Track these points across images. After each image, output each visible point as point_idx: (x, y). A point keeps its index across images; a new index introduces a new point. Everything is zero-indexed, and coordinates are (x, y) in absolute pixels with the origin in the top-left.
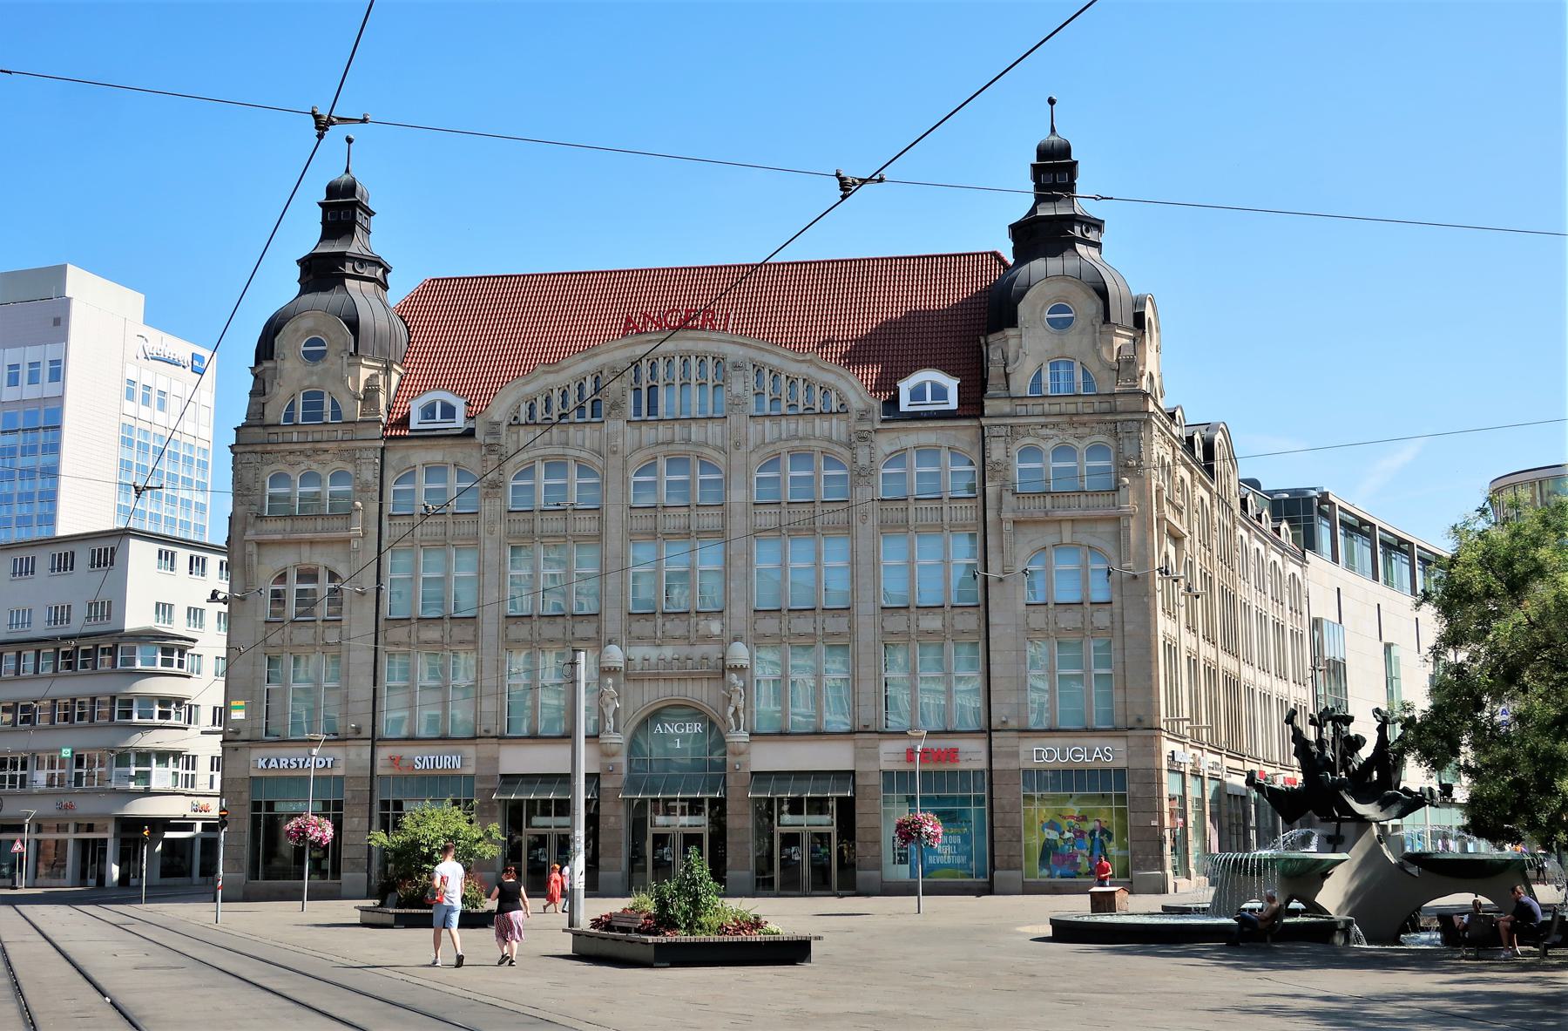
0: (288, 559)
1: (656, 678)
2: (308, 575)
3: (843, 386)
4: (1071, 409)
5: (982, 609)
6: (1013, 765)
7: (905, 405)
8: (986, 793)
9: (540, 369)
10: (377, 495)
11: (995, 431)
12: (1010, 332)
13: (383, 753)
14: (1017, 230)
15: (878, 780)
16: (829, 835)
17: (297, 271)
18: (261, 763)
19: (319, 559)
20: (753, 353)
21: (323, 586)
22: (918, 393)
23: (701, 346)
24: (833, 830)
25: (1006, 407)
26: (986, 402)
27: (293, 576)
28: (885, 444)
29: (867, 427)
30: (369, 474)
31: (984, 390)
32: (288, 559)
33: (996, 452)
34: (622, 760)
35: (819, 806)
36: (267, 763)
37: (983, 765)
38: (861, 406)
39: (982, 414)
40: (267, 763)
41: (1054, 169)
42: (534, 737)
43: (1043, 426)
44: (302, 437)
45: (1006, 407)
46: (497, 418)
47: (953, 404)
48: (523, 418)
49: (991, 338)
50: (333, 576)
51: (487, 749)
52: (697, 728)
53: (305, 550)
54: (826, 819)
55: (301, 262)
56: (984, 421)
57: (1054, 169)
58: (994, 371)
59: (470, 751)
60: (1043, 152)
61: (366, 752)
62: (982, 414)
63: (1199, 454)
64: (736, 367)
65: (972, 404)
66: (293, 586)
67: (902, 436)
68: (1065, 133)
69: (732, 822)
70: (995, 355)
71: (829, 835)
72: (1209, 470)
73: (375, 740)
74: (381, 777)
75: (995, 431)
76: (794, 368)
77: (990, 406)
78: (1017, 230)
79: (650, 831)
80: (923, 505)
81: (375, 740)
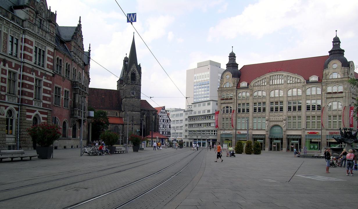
0: (225, 105)
1: (273, 121)
2: (227, 107)
3: (300, 78)
4: (336, 80)
6: (325, 134)
8: (321, 138)
10: (236, 96)
11: (324, 84)
12: (327, 69)
13: (237, 131)
14: (329, 52)
17: (226, 66)
18: (222, 132)
19: (229, 105)
20: (287, 74)
21: (229, 109)
23: (280, 73)
25: (326, 81)
27: (225, 108)
28: (307, 87)
29: (304, 84)
30: (235, 94)
32: (225, 105)
33: (324, 87)
34: (268, 133)
37: (321, 134)
41: (336, 41)
42: (257, 130)
43: (332, 83)
44: (226, 89)
45: (326, 81)
46: (252, 85)
50: (231, 108)
52: (279, 128)
53: (227, 104)
54: (298, 141)
55: (226, 65)
58: (324, 76)
60: (334, 39)
64: (285, 76)
65: (320, 81)
66: (225, 109)
67: (310, 85)
69: (284, 142)
70: (324, 72)
75: (324, 84)
76: (293, 76)
78: (329, 52)
80: (313, 96)
81: (236, 130)
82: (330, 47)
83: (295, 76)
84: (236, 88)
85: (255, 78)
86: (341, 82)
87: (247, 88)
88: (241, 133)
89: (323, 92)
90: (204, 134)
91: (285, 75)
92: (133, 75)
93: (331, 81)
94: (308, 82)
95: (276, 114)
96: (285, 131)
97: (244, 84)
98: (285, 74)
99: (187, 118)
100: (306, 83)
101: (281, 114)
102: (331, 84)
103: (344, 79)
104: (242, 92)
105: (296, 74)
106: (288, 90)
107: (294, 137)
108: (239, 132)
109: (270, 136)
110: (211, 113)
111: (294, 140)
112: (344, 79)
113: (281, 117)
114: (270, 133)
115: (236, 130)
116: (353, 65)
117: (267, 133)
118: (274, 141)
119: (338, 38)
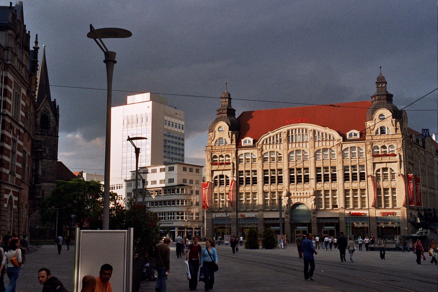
5: (366, 182)
7: (348, 137)
9: (269, 132)
11: (368, 143)
13: (239, 214)
15: (343, 219)
16: (334, 230)
18: (214, 216)
22: (351, 135)
24: (335, 230)
26: (366, 137)
31: (366, 134)
35: (331, 224)
36: (215, 216)
38: (338, 138)
39: (365, 140)
40: (215, 216)
41: (381, 81)
43: (379, 142)
44: (220, 148)
47: (358, 136)
48: (265, 143)
49: (367, 122)
50: (227, 177)
51: (261, 213)
54: (333, 227)
56: (366, 141)
57: (381, 81)
59: (256, 213)
60: (378, 78)
61: (235, 214)
62: (365, 140)
63: (421, 143)
68: (383, 75)
71: (334, 230)
72: (424, 147)
73: (237, 211)
74: (239, 219)
77: (367, 138)
79: (296, 230)
82: (373, 90)
83: (325, 130)
84: (234, 147)
85: (266, 132)
86: (393, 140)
87: (254, 146)
88: (247, 216)
89: (368, 153)
90: (165, 219)
91: (310, 129)
92: (45, 119)
93: (378, 138)
94: (345, 139)
95: (299, 186)
96: (314, 212)
97: (248, 140)
98: (310, 127)
99: (131, 191)
100: (342, 140)
101: (306, 186)
102: (380, 143)
103: (396, 136)
104: (245, 153)
105: (326, 128)
106: (315, 150)
107: (329, 221)
108: (242, 215)
109: (291, 219)
110: (175, 183)
111: (327, 225)
112: (396, 136)
113: (308, 191)
114: (291, 216)
115: (237, 211)
116: (405, 116)
117: (287, 215)
118: (298, 228)
119: (383, 78)
